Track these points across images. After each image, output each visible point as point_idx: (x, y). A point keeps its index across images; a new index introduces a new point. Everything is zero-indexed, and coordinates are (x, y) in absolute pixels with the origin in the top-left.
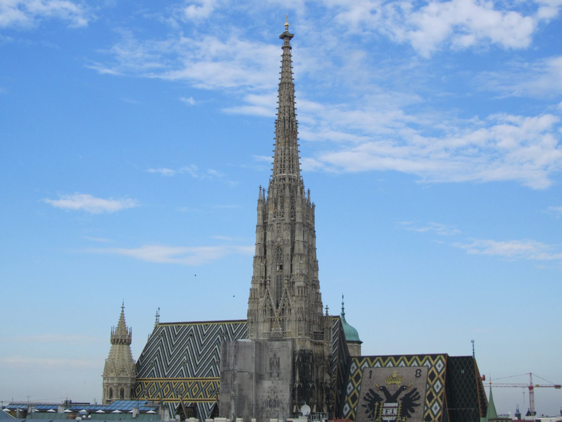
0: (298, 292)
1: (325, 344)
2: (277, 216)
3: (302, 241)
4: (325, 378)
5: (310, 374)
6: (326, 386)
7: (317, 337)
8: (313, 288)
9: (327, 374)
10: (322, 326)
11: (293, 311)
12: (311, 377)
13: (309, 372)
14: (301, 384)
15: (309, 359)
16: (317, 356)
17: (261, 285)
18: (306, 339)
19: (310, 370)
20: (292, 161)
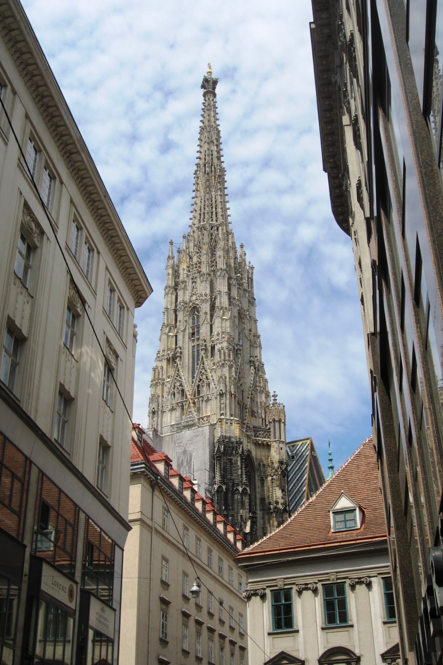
0: (219, 356)
1: (272, 444)
2: (193, 269)
3: (226, 293)
4: (274, 495)
5: (240, 473)
6: (276, 508)
7: (260, 434)
8: (251, 366)
9: (277, 488)
10: (267, 420)
11: (212, 385)
12: (242, 477)
13: (238, 469)
14: (224, 487)
15: (236, 450)
16: (262, 464)
17: (168, 360)
18: (232, 420)
19: (240, 467)
20: (216, 209)
